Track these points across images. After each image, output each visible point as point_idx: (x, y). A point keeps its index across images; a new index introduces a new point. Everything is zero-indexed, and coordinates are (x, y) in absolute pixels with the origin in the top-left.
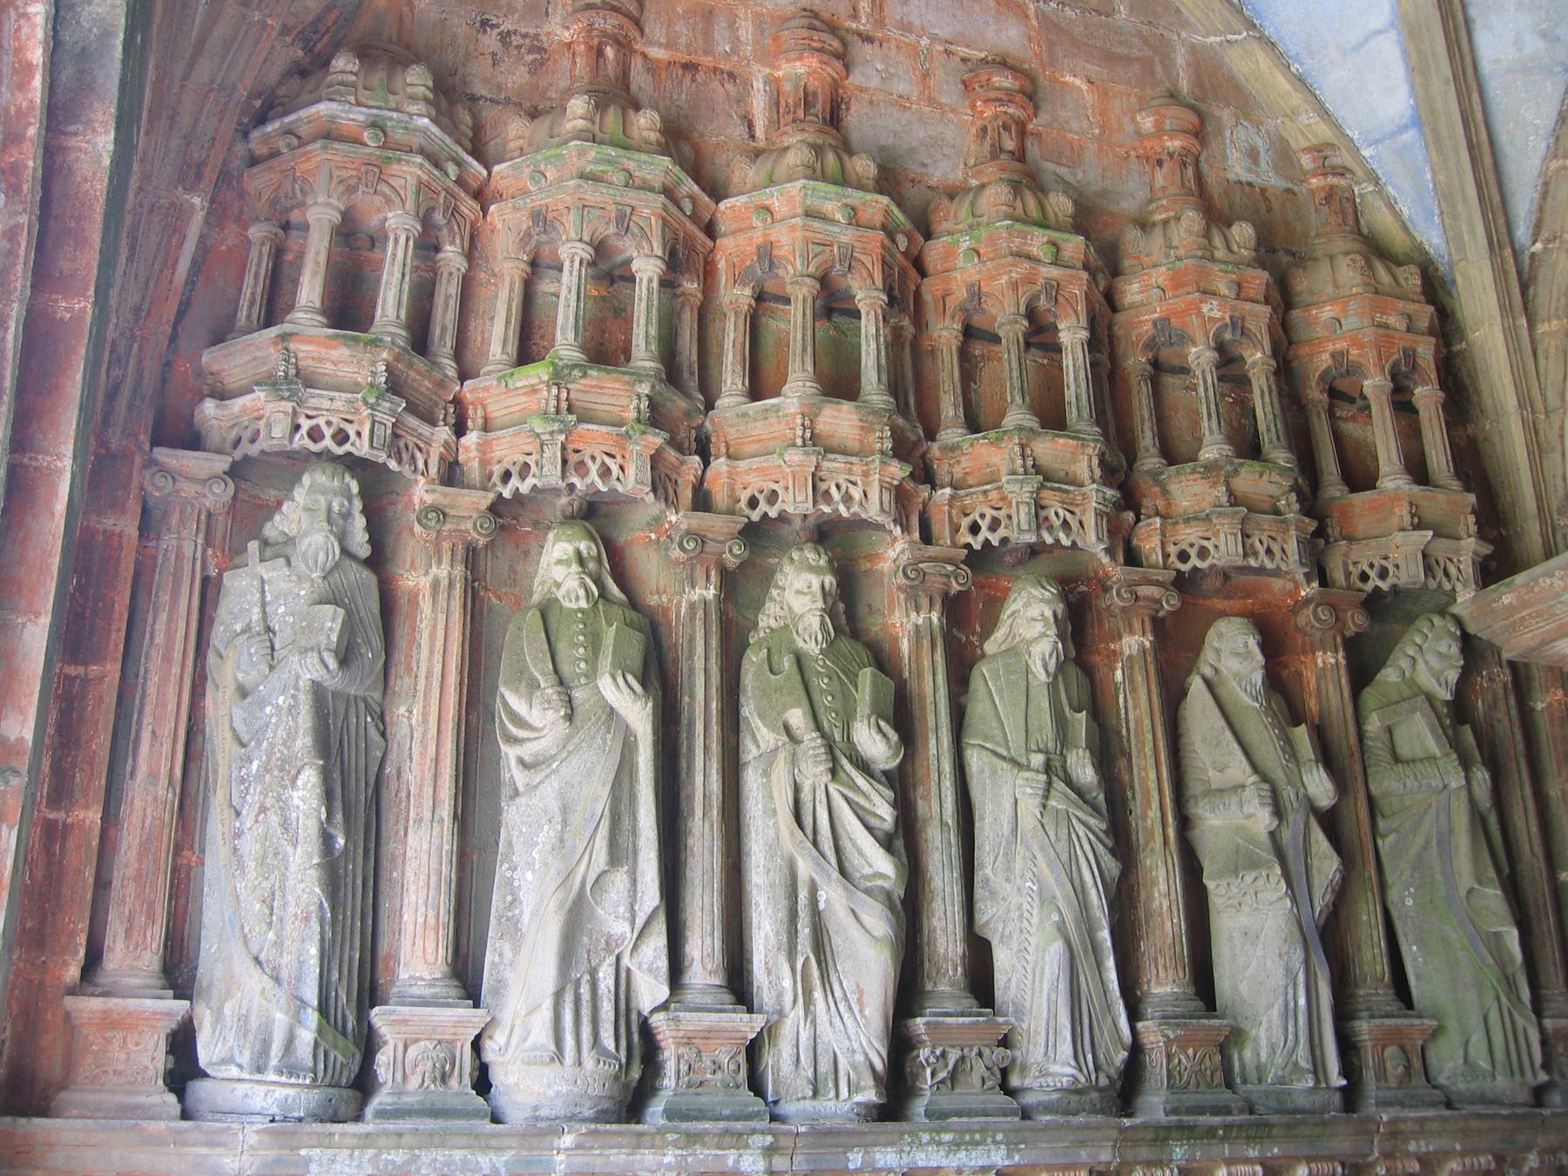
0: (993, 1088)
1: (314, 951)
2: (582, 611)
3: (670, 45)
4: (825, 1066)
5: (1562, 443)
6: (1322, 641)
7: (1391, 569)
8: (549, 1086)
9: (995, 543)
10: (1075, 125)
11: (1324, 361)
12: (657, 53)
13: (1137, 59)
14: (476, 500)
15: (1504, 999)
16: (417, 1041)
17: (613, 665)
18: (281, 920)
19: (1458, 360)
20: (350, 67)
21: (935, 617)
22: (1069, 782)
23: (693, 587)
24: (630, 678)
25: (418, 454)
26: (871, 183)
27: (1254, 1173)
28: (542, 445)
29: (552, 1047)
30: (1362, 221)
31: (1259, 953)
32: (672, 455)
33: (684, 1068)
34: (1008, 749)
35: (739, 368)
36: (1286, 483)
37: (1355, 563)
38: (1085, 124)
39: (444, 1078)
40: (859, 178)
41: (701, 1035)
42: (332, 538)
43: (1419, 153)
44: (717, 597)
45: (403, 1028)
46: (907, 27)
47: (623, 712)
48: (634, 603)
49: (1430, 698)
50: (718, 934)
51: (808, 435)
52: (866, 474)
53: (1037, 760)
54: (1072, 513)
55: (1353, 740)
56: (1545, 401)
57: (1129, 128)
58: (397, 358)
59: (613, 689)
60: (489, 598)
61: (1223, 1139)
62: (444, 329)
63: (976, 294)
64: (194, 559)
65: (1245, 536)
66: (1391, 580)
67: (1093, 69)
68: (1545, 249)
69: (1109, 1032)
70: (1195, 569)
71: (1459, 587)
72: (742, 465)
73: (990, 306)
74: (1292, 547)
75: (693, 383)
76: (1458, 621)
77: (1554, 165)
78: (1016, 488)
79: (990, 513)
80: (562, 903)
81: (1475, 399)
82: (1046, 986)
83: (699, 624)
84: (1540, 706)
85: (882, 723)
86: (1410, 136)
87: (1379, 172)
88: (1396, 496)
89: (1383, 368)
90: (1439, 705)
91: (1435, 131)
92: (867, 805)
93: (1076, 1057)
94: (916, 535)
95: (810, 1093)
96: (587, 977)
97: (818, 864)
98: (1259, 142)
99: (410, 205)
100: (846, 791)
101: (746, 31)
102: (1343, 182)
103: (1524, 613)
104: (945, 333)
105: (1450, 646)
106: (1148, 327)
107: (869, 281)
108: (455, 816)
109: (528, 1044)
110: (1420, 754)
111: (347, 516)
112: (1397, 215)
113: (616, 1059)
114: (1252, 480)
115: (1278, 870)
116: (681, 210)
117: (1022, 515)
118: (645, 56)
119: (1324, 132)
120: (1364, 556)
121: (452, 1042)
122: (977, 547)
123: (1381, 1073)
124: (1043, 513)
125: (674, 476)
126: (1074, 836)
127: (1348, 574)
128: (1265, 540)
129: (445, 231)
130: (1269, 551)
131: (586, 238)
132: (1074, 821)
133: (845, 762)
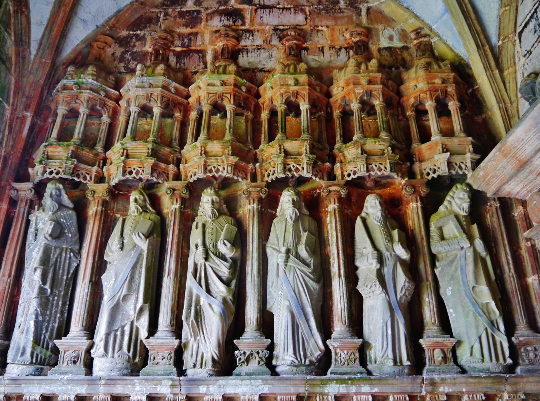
0: (263, 365)
1: (32, 323)
3: (183, 45)
4: (199, 358)
5: (518, 113)
6: (412, 199)
7: (437, 169)
9: (274, 179)
10: (321, 42)
11: (412, 100)
12: (178, 49)
13: (346, 17)
15: (489, 331)
16: (68, 350)
18: (27, 315)
19: (477, 92)
20: (71, 69)
21: (255, 205)
22: (297, 256)
23: (173, 204)
24: (140, 234)
25: (87, 175)
26: (233, 72)
27: (368, 399)
28: (118, 167)
30: (435, 51)
31: (376, 314)
32: (163, 165)
33: (152, 358)
34: (279, 246)
35: (191, 137)
36: (387, 144)
37: (425, 170)
38: (325, 41)
39: (75, 362)
40: (230, 71)
42: (53, 202)
43: (451, 22)
44: (180, 208)
45: (63, 347)
46: (261, 24)
47: (140, 245)
48: (159, 212)
49: (457, 217)
50: (169, 314)
51: (203, 152)
52: (223, 162)
53: (283, 249)
54: (300, 165)
55: (423, 233)
56: (510, 99)
57: (342, 39)
58: (77, 148)
61: (352, 384)
62: (100, 139)
63: (272, 100)
64: (24, 213)
65: (368, 164)
66: (437, 173)
67: (329, 23)
68: (503, 43)
69: (313, 344)
70: (353, 179)
71: (466, 172)
72: (187, 165)
73: (275, 103)
74: (388, 166)
75: (176, 144)
76: (469, 185)
77: (502, 10)
78: (276, 159)
79: (272, 169)
81: (484, 104)
82: (283, 328)
84: (516, 214)
85: (226, 241)
86: (447, 16)
87: (440, 32)
88: (436, 143)
89: (432, 99)
90: (461, 217)
91: (451, 11)
92: (219, 269)
93: (295, 353)
94: (249, 180)
95: (192, 366)
96: (120, 329)
97: (198, 289)
98: (393, 33)
99: (85, 105)
100: (211, 265)
101: (207, 37)
102: (426, 39)
103: (489, 177)
104: (264, 115)
105: (464, 195)
106: (339, 101)
107: (228, 102)
108: (91, 281)
110: (452, 235)
111: (60, 195)
112: (448, 46)
114: (372, 145)
115: (378, 283)
116: (170, 91)
117: (279, 168)
118: (174, 51)
119: (418, 24)
120: (427, 166)
121: (79, 350)
122: (270, 181)
123: (432, 360)
124: (288, 167)
125: (166, 172)
126: (296, 275)
127: (422, 174)
128: (377, 164)
129: (103, 111)
130: (380, 169)
131: (137, 105)
132: (297, 270)
133: (212, 255)
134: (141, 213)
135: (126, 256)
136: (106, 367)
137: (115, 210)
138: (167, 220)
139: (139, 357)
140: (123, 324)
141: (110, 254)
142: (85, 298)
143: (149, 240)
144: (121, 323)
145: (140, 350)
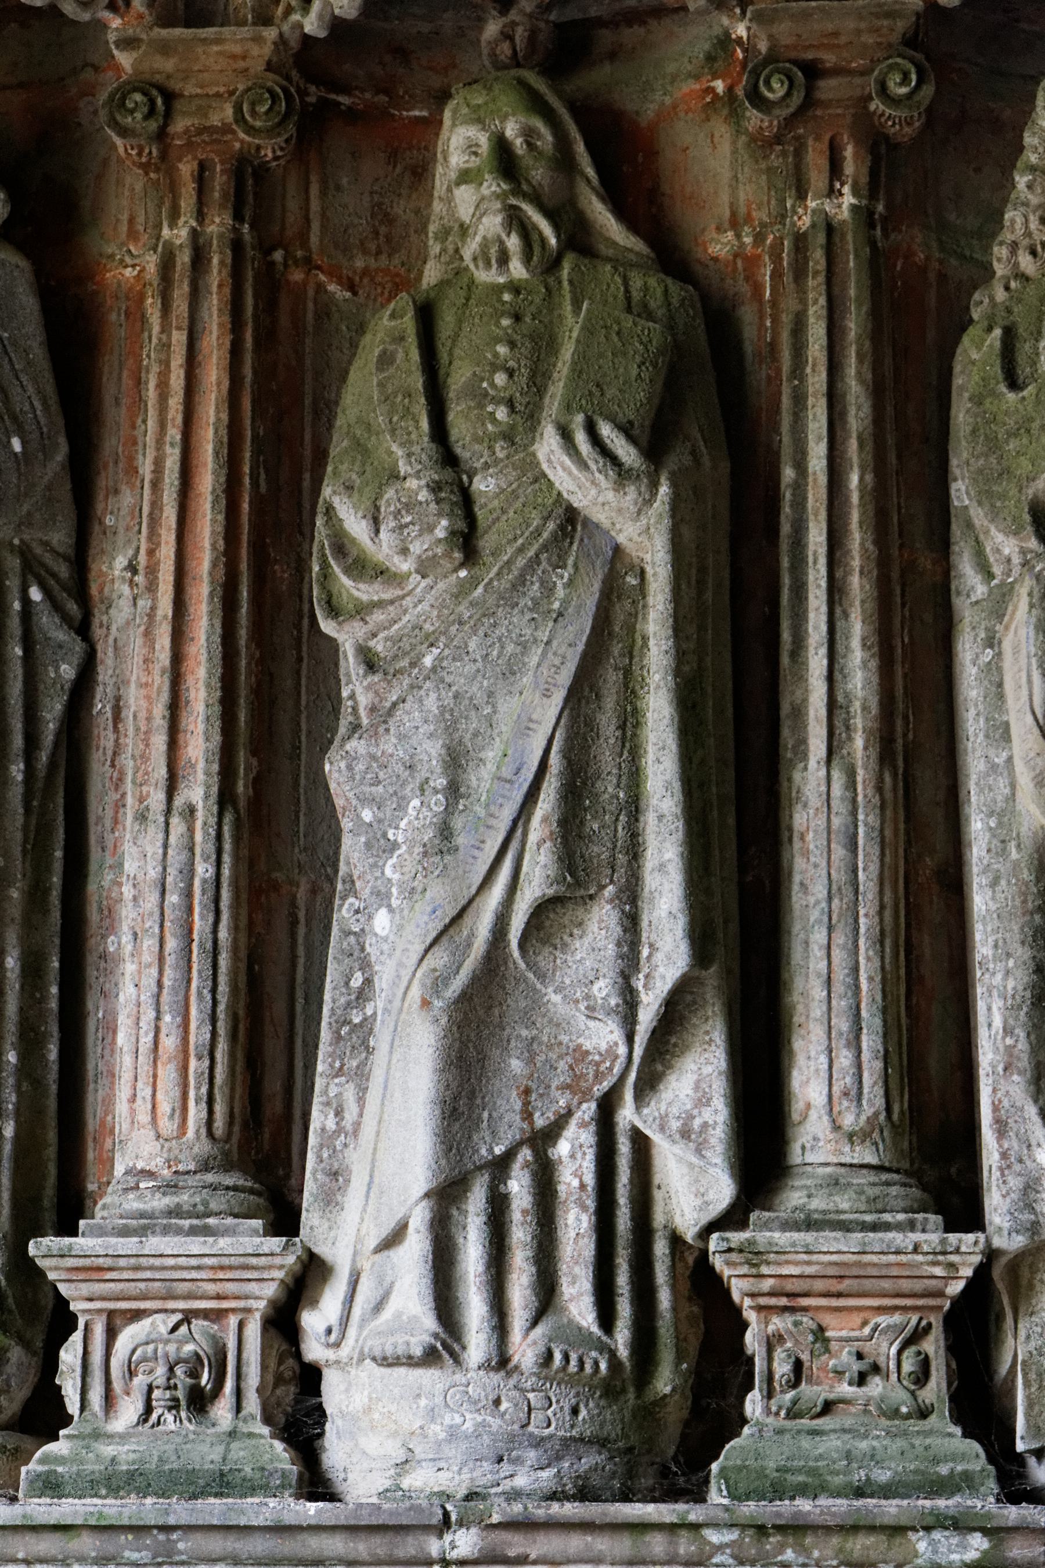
2: (515, 288)
8: (432, 1414)
14: (237, 49)
16: (137, 1315)
17: (568, 407)
23: (801, 196)
24: (606, 430)
29: (430, 1323)
33: (782, 1368)
41: (819, 1285)
44: (864, 215)
47: (600, 516)
50: (871, 1042)
59: (568, 462)
60: (320, 288)
80: (438, 982)
83: (815, 284)
96: (526, 1154)
108: (225, 798)
109: (387, 1314)
113: (602, 1348)
121: (216, 1315)
134: (553, 265)
135: (509, 598)
136: (453, 1434)
137: (314, 239)
138: (747, 314)
139: (680, 1358)
140: (540, 1122)
141: (363, 591)
142: (200, 924)
143: (674, 485)
144: (527, 1115)
145: (674, 1309)
